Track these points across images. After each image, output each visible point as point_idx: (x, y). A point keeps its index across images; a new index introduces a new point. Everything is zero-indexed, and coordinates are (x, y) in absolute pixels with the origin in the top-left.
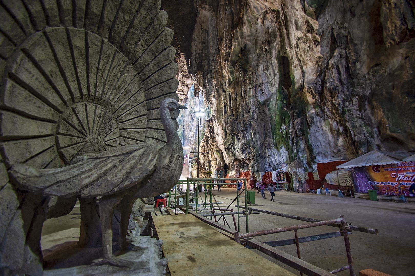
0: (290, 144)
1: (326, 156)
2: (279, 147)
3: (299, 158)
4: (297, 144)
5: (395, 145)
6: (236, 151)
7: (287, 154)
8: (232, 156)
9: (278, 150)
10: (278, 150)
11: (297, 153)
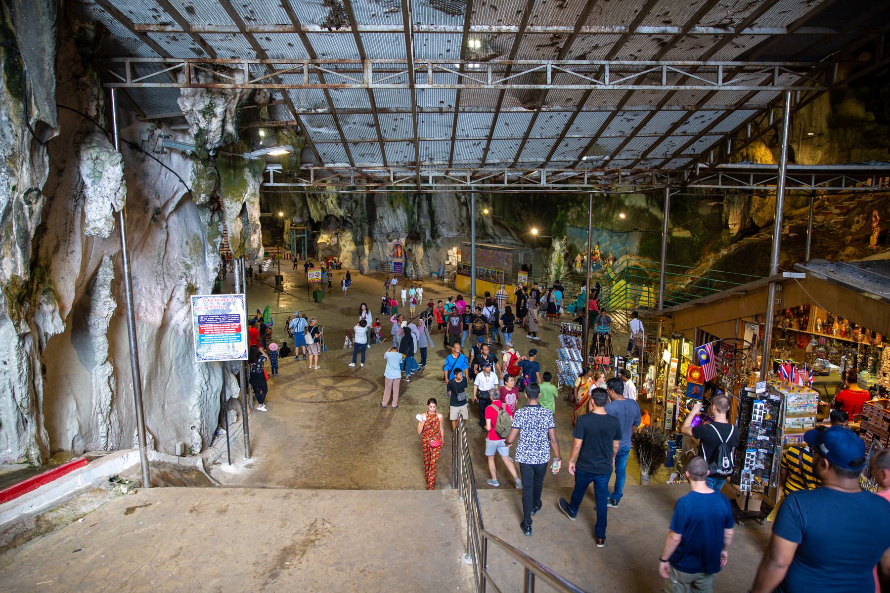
0: (411, 203)
1: (451, 229)
2: (395, 204)
3: (420, 227)
4: (419, 206)
5: (505, 231)
6: (329, 200)
7: (406, 218)
8: (322, 208)
9: (394, 211)
10: (394, 211)
11: (419, 220)
